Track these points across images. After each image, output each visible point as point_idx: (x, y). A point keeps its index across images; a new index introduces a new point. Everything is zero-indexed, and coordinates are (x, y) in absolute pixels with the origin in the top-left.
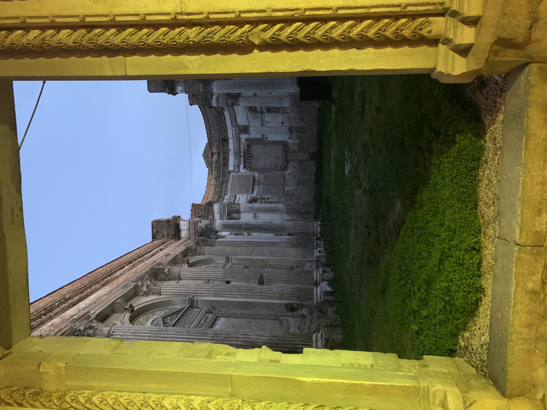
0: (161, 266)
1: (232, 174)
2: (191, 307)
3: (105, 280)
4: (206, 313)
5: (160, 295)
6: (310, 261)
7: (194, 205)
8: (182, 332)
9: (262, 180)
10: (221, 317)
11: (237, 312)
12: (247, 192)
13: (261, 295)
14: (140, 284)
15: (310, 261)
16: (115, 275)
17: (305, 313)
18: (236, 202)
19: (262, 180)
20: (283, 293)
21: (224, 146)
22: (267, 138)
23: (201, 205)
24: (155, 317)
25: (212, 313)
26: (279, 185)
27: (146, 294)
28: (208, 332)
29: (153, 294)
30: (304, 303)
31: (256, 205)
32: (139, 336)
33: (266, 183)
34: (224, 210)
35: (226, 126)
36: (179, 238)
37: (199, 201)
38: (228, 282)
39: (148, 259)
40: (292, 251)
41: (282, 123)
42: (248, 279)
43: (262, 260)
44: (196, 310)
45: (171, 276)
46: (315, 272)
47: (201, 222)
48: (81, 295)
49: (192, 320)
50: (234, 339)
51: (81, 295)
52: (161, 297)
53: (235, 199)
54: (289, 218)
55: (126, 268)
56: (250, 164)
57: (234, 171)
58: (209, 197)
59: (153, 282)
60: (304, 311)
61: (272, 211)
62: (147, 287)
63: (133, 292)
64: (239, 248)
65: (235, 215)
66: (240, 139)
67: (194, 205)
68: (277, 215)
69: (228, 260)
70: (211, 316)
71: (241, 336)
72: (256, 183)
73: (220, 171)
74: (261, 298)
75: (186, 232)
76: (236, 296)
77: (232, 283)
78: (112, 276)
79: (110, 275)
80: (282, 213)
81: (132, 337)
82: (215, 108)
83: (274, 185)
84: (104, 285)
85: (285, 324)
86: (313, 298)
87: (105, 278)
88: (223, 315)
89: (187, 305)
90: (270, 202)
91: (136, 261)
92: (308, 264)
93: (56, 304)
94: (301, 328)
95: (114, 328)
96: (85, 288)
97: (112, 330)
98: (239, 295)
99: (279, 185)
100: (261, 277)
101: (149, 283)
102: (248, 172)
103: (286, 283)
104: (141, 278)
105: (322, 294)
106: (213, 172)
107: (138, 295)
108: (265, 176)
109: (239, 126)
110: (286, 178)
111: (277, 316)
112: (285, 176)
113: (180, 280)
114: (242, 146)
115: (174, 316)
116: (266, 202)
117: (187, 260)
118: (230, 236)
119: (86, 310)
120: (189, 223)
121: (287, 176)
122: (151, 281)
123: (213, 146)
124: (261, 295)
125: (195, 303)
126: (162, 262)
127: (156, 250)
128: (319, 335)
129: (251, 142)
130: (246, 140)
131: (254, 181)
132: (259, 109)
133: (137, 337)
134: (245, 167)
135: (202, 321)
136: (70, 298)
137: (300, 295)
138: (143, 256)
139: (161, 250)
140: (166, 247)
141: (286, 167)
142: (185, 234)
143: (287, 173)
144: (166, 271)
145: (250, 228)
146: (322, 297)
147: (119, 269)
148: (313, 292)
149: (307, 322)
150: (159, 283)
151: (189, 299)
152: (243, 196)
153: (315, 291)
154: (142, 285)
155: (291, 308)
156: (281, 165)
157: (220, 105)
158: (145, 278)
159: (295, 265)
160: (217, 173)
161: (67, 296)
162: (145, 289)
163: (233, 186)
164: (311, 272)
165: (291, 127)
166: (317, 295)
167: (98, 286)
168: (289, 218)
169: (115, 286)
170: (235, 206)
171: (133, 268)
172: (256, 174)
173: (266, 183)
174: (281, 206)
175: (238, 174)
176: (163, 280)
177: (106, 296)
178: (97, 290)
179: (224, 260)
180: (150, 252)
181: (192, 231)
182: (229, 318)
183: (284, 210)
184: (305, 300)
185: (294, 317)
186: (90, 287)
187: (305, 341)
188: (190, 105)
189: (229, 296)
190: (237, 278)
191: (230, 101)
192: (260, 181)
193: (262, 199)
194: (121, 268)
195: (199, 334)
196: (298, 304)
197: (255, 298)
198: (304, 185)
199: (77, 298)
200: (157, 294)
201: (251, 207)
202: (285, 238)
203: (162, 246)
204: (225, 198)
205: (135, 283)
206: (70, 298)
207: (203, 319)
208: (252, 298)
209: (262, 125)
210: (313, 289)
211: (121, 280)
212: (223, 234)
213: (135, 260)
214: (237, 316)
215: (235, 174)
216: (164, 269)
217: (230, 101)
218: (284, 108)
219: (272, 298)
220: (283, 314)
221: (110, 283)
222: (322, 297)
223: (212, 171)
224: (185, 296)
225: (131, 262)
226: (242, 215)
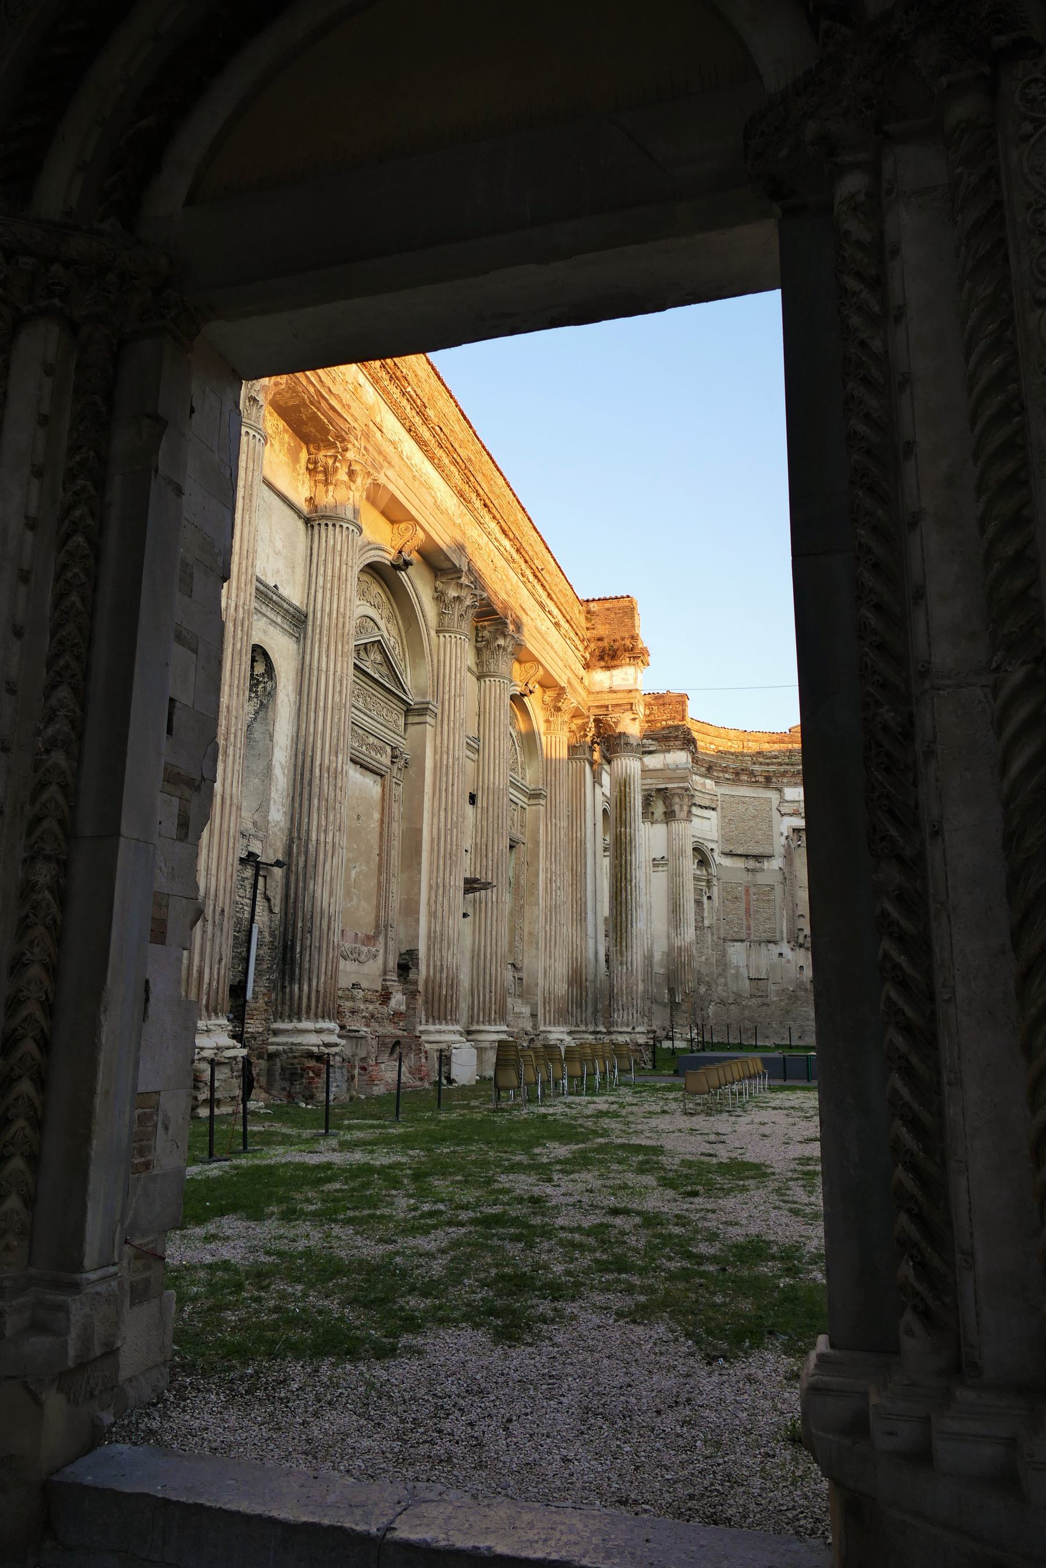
0: (511, 627)
1: (774, 796)
2: (409, 711)
3: (474, 496)
4: (393, 748)
5: (437, 632)
6: (534, 1016)
7: (682, 700)
8: (340, 692)
9: (761, 879)
10: (383, 787)
11: (395, 825)
12: (726, 839)
13: (437, 886)
14: (464, 580)
15: (534, 1016)
16: (488, 518)
17: (393, 1003)
19: (761, 879)
20: (445, 944)
23: (683, 718)
24: (382, 623)
25: (393, 762)
26: (749, 928)
27: (439, 597)
28: (340, 756)
29: (441, 614)
30: (420, 1000)
31: (689, 866)
32: (332, 590)
33: (753, 890)
34: (671, 779)
36: (587, 666)
37: (696, 711)
38: (473, 799)
39: (533, 595)
40: (561, 969)
42: (481, 851)
43: (535, 886)
44: (401, 722)
45: (486, 655)
46: (505, 1028)
47: (634, 719)
48: (432, 443)
49: (373, 714)
50: (324, 823)
51: (432, 443)
52: (433, 633)
53: (706, 808)
54: (657, 956)
55: (506, 543)
57: (783, 801)
58: (709, 739)
59: (471, 611)
60: (398, 1000)
61: (675, 908)
62: (458, 599)
63: (445, 565)
64: (564, 824)
65: (659, 809)
67: (682, 700)
68: (665, 921)
69: (535, 795)
70: (386, 760)
71: (329, 839)
72: (752, 864)
73: (780, 764)
74: (431, 887)
75: (606, 685)
76: (435, 821)
77: (469, 808)
78: (484, 512)
79: (485, 505)
80: (668, 937)
81: (330, 573)
83: (747, 910)
84: (461, 495)
85: (365, 949)
86: (434, 1024)
87: (478, 495)
88: (387, 790)
89: (412, 699)
90: (699, 903)
91: (523, 566)
92: (526, 1010)
93: (409, 389)
94: (355, 992)
95: (351, 528)
96: (451, 450)
97: (345, 525)
98: (439, 829)
100: (486, 886)
101: (468, 602)
102: (783, 841)
103: (473, 951)
104: (478, 582)
105: (443, 1046)
106: (777, 746)
107: (436, 577)
108: (772, 888)
110: (771, 946)
111: (386, 927)
112: (775, 943)
113: (478, 679)
115: (384, 670)
116: (698, 891)
117: (531, 692)
118: (599, 798)
119: (395, 460)
120: (630, 691)
121: (775, 949)
122: (473, 606)
124: (437, 886)
125: (417, 719)
126: (525, 630)
127: (556, 612)
128: (334, 1039)
131: (758, 858)
133: (329, 585)
135: (371, 740)
136: (425, 420)
137: (440, 987)
138: (539, 580)
139: (557, 625)
140: (564, 637)
141: (801, 946)
142: (602, 682)
143: (785, 948)
144: (501, 642)
145: (620, 850)
146: (435, 1046)
147: (501, 527)
148: (447, 1023)
149: (371, 1007)
150: (467, 627)
151: (428, 703)
152: (715, 828)
153: (451, 1028)
154: (461, 586)
155: (406, 965)
158: (478, 592)
159: (524, 975)
160: (776, 757)
161: (430, 413)
162: (452, 593)
163: (742, 800)
164: (502, 1015)
166: (440, 1032)
167: (457, 479)
168: (657, 956)
169: (458, 521)
170: (686, 808)
171: (506, 560)
172: (777, 863)
174: (690, 933)
175: (775, 814)
176: (477, 635)
177: (430, 500)
178: (447, 478)
179: (532, 787)
180: (549, 595)
181: (609, 700)
182: (379, 808)
183: (678, 942)
184: (426, 1002)
185: (385, 973)
186: (455, 462)
187: (317, 1001)
189: (436, 803)
190: (484, 823)
192: (759, 875)
193: (708, 881)
194: (504, 532)
195: (335, 734)
196: (416, 983)
197: (431, 872)
198: (752, 996)
199: (426, 435)
200: (440, 623)
201: (682, 852)
202: (597, 945)
203: (566, 626)
204: (708, 782)
205: (465, 569)
206: (425, 420)
207: (376, 742)
208: (431, 864)
210: (457, 1022)
211: (474, 532)
212: (606, 779)
213: (526, 562)
214: (385, 826)
215: (775, 803)
216: (505, 636)
219: (432, 915)
220: (390, 943)
221: (467, 507)
222: (435, 1046)
224: (436, 694)
225: (518, 550)
226: (660, 829)
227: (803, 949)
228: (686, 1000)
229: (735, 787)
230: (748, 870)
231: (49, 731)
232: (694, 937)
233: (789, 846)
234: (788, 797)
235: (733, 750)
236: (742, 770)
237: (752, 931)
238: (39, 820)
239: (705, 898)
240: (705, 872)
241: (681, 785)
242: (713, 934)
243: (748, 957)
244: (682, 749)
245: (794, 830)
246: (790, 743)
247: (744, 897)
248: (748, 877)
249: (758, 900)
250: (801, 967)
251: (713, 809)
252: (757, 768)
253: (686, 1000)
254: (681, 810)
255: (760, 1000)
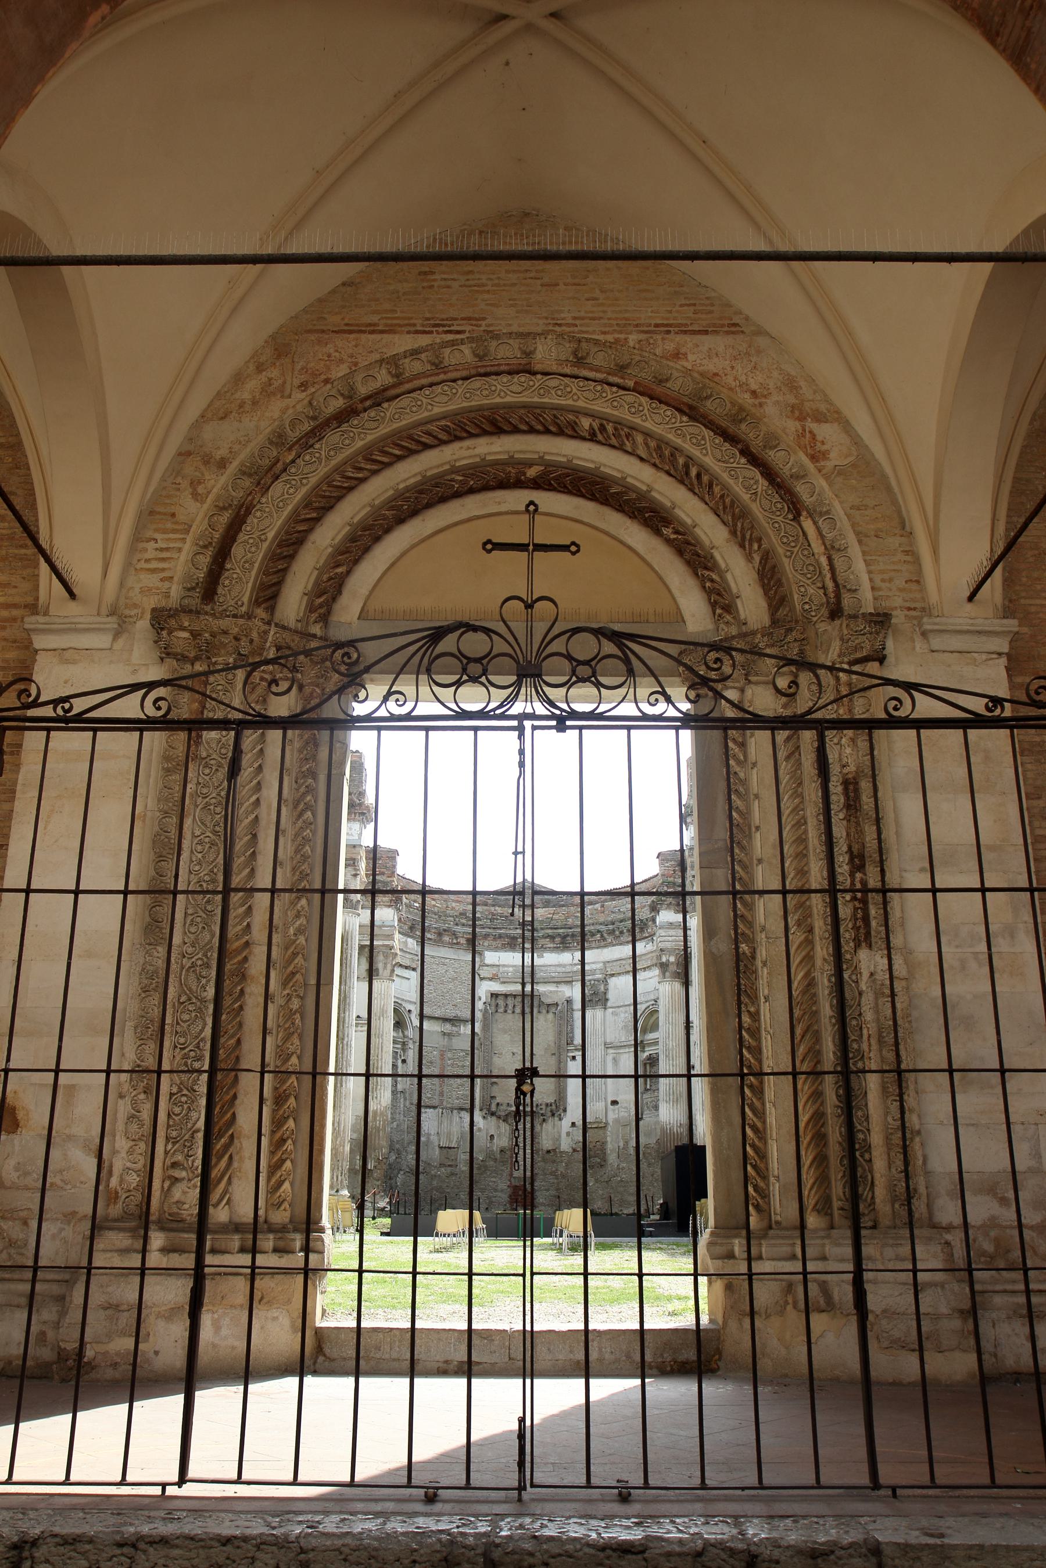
18: (398, 971)
21: (552, 938)
22: (574, 1058)
26: (441, 1094)
35: (605, 946)
41: (614, 1103)
53: (406, 968)
56: (501, 1010)
66: (569, 982)
72: (448, 1027)
82: (654, 920)
99: (441, 1094)
109: (605, 981)
114: (551, 988)
120: (354, 846)
123: (552, 910)
129: (562, 1011)
130: (569, 1002)
132: (651, 1036)
134: (494, 995)
141: (493, 1114)
156: (498, 1100)
157: (662, 932)
165: (606, 1124)
170: (389, 967)
173: (449, 1055)
188: (659, 854)
191: (672, 959)
192: (454, 1040)
198: (442, 1165)
204: (410, 940)
209: (607, 1046)
217: (672, 959)
218: (656, 1108)
223: (486, 905)
227: (494, 1118)
228: (379, 1167)
229: (436, 948)
230: (444, 1034)
231: (298, 923)
232: (389, 1102)
233: (486, 1008)
234: (487, 961)
235: (436, 909)
236: (445, 930)
237: (445, 1098)
238: (293, 974)
239: (400, 1061)
240: (401, 1034)
241: (386, 943)
242: (405, 1099)
243: (440, 1123)
244: (389, 906)
245: (492, 995)
246: (493, 906)
247: (438, 1061)
248: (445, 1041)
249: (452, 1065)
250: (492, 1136)
251: (414, 969)
252: (459, 929)
253: (379, 1167)
254: (385, 968)
255: (449, 1169)
